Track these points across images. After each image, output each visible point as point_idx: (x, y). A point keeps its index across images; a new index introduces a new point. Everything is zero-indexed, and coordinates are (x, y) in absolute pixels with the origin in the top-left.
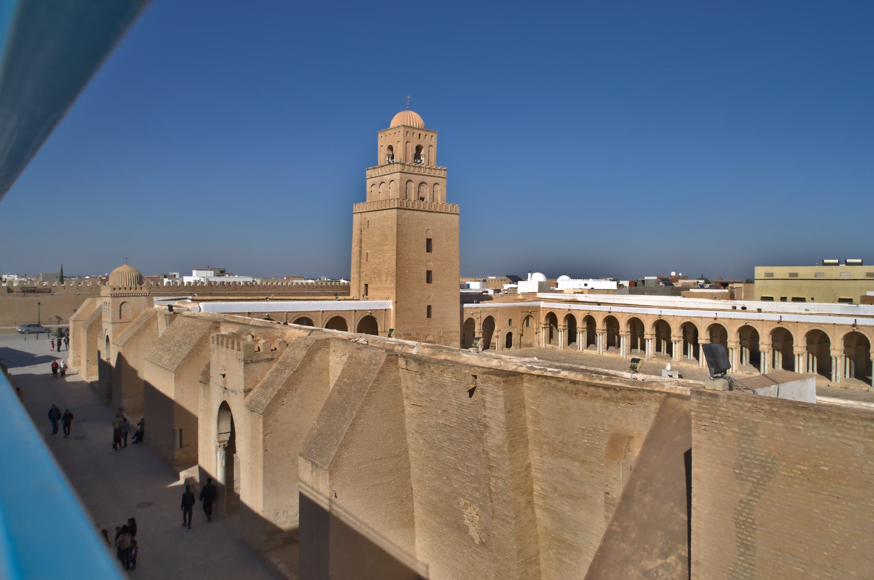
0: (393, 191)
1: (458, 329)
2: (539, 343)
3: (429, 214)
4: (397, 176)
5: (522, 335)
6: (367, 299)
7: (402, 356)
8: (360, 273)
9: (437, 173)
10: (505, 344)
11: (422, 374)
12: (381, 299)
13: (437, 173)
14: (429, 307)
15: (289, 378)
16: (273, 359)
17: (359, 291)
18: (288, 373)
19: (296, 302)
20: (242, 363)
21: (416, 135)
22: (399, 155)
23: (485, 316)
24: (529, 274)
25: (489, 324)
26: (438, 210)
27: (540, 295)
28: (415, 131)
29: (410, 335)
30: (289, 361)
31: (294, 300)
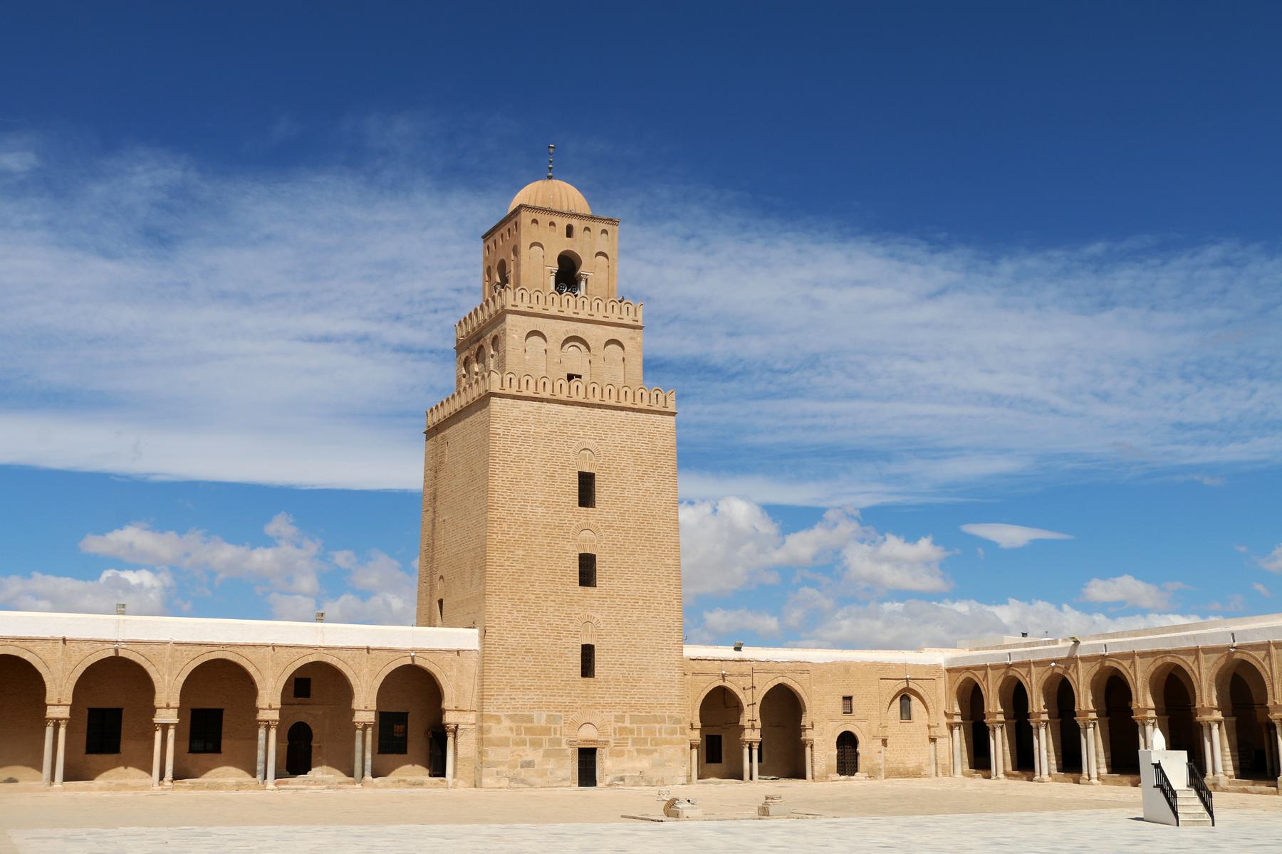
3: (587, 410)
10: (834, 762)
23: (766, 684)
28: (556, 219)
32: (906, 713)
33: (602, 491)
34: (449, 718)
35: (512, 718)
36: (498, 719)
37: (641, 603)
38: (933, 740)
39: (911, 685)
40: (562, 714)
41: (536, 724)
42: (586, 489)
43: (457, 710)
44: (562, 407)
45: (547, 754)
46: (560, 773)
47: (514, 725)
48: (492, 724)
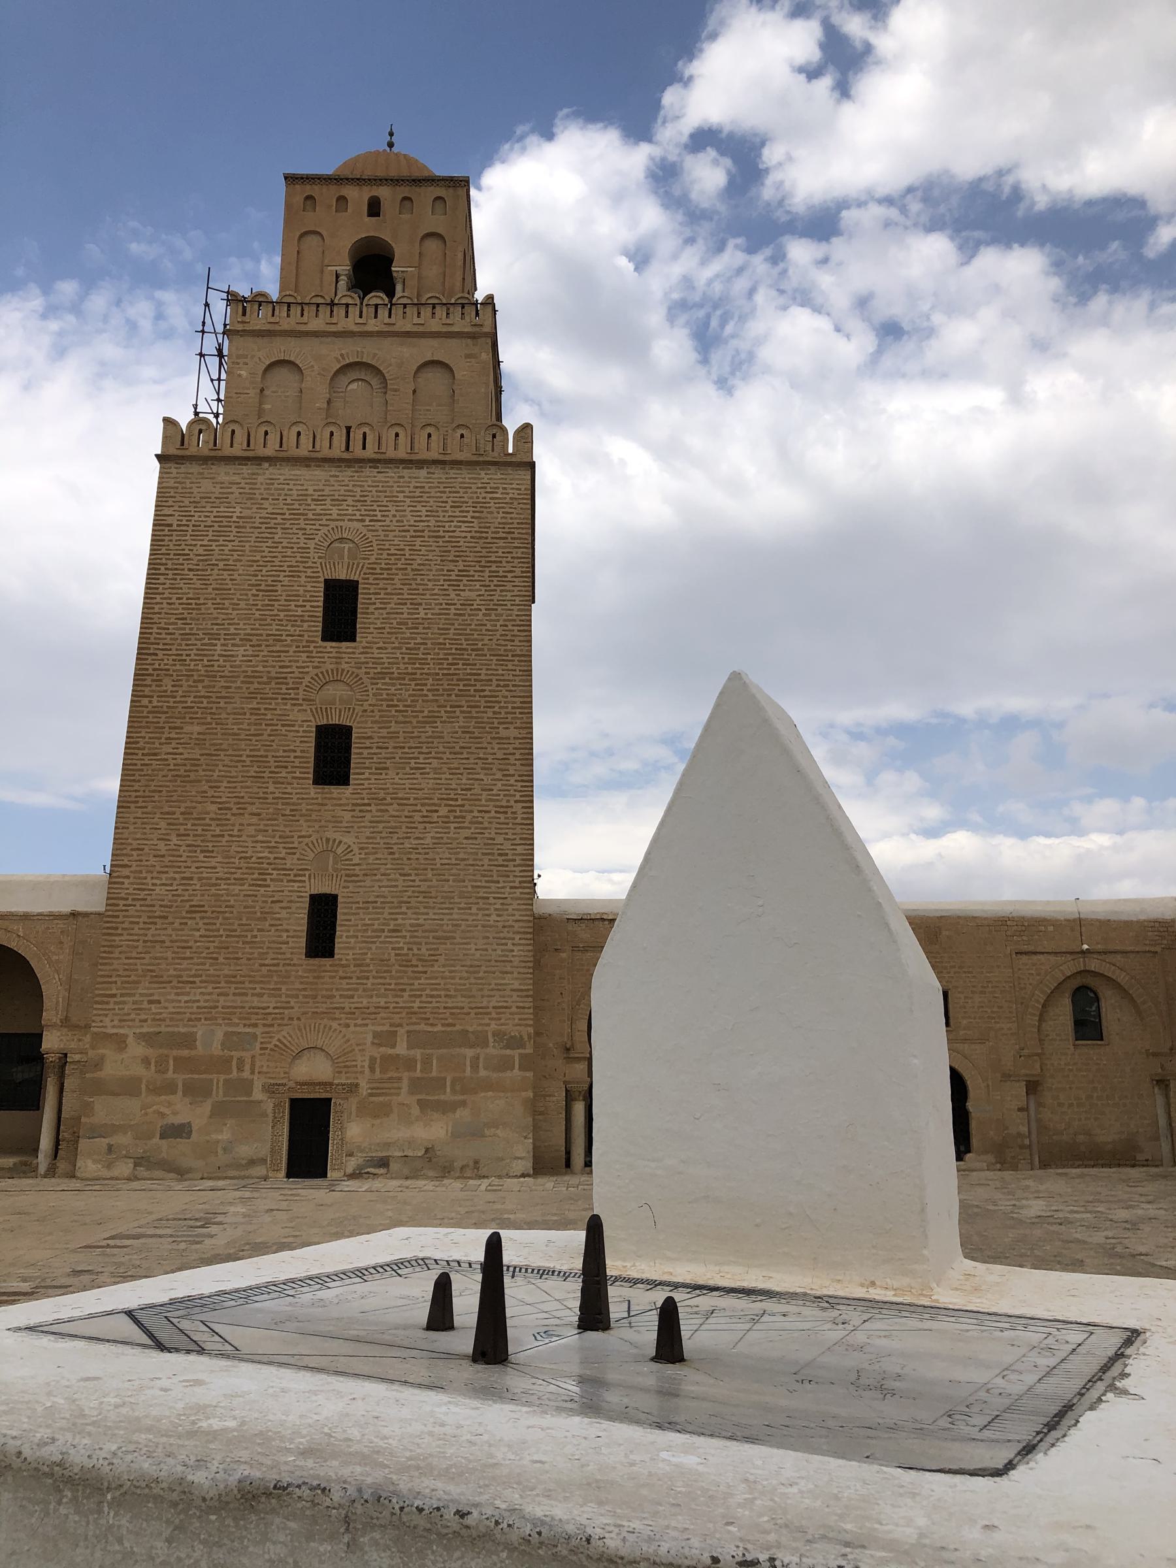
3: (346, 474)
29: (188, 1041)
32: (1088, 1026)
33: (370, 616)
34: (51, 1042)
36: (120, 1043)
38: (1162, 1083)
39: (1094, 965)
40: (258, 1031)
41: (200, 1050)
42: (340, 611)
43: (66, 1023)
44: (301, 472)
45: (220, 1112)
46: (245, 1151)
47: (151, 1052)
48: (108, 1052)
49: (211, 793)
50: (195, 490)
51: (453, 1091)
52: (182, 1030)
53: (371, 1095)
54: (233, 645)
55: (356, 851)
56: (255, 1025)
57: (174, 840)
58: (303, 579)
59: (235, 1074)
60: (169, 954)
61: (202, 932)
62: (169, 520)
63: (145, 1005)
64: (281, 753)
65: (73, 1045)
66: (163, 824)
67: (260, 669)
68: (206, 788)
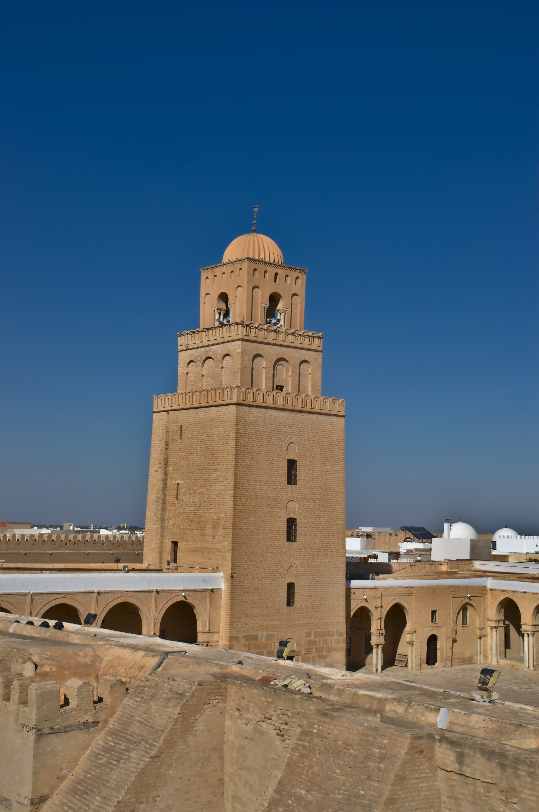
0: (230, 374)
1: (342, 627)
2: (486, 657)
3: (292, 415)
4: (237, 347)
5: (454, 641)
6: (176, 569)
7: (443, 739)
8: (163, 520)
9: (307, 342)
10: (425, 656)
11: (509, 793)
12: (203, 569)
13: (307, 342)
14: (291, 587)
15: (142, 773)
16: (96, 723)
17: (161, 554)
18: (137, 759)
19: (46, 575)
20: (32, 735)
21: (270, 276)
22: (238, 310)
23: (388, 605)
24: (446, 526)
25: (396, 618)
26: (308, 408)
27: (479, 565)
28: (269, 268)
29: (256, 638)
30: (135, 728)
31: (42, 570)
35: (246, 638)
37: (322, 551)
47: (247, 643)
49: (258, 544)
50: (247, 419)
51: (326, 652)
52: (254, 633)
53: (305, 654)
54: (262, 485)
55: (299, 567)
56: (274, 631)
57: (248, 562)
58: (281, 459)
59: (269, 649)
60: (250, 606)
61: (259, 598)
62: (241, 431)
63: (244, 625)
64: (277, 529)
65: (211, 640)
66: (245, 557)
67: (270, 495)
68: (257, 542)
